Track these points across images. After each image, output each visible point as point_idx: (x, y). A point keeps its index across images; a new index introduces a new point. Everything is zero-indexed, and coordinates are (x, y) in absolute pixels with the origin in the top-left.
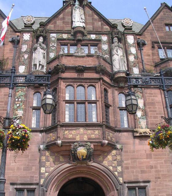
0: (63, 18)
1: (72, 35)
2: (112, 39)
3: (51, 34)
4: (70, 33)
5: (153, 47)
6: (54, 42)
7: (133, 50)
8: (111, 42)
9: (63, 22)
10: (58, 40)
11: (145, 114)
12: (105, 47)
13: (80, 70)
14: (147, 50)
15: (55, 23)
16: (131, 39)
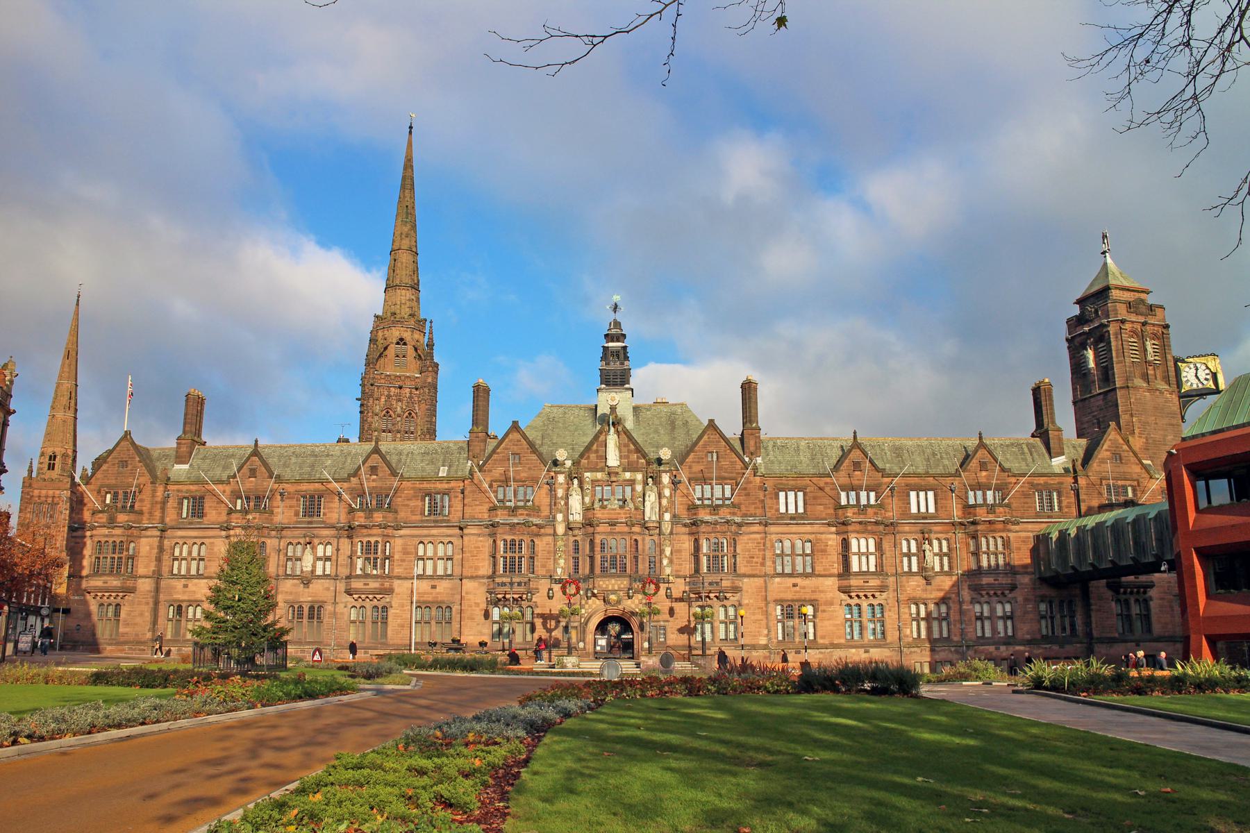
0: (597, 451)
7: (667, 492)
11: (671, 561)
12: (639, 488)
16: (666, 479)
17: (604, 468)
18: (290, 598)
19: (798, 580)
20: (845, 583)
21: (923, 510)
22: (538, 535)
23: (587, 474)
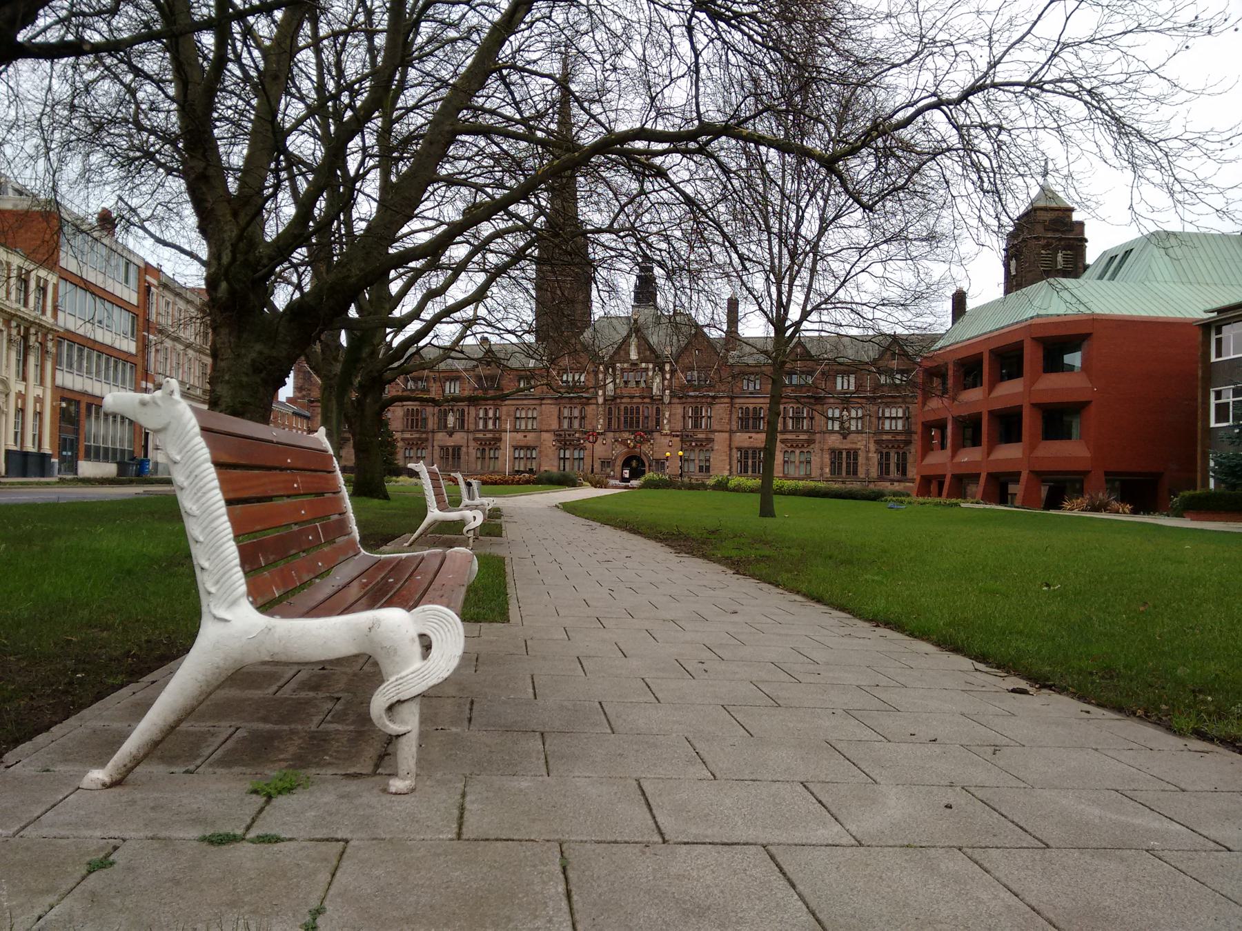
7: (668, 376)
11: (669, 421)
17: (628, 360)
18: (441, 443)
19: (753, 435)
21: (845, 387)
22: (588, 404)
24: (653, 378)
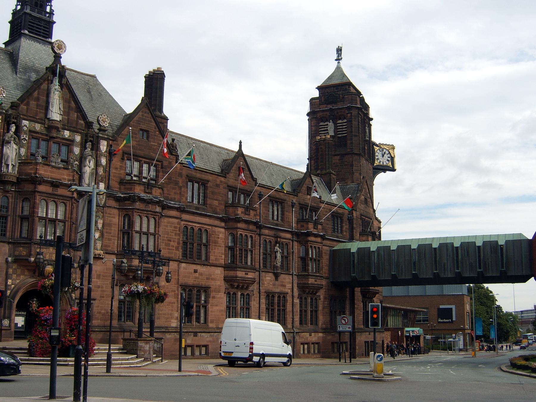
0: (38, 99)
1: (45, 128)
2: (86, 142)
3: (24, 121)
4: (44, 124)
5: (123, 159)
6: (25, 133)
7: (104, 161)
8: (83, 147)
9: (37, 105)
10: (30, 131)
12: (77, 150)
13: (55, 185)
14: (116, 161)
15: (28, 104)
17: (45, 119)
19: (198, 267)
20: (231, 273)
23: (25, 123)
24: (82, 159)
